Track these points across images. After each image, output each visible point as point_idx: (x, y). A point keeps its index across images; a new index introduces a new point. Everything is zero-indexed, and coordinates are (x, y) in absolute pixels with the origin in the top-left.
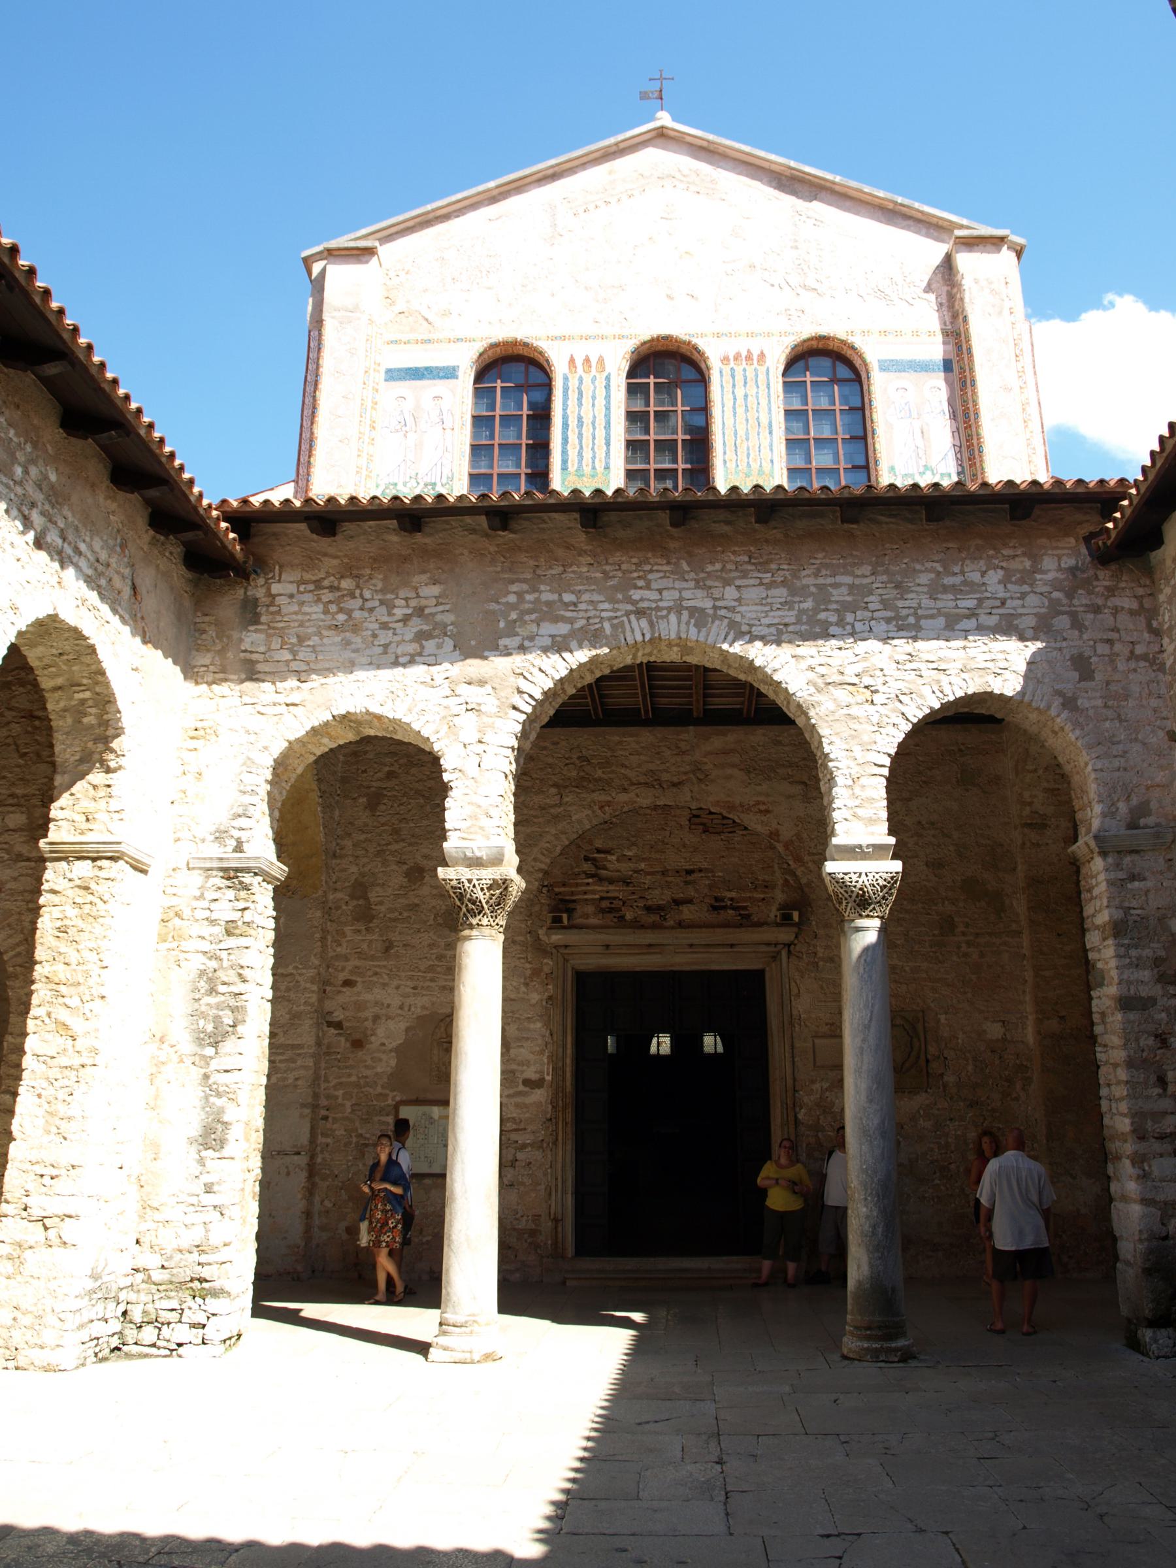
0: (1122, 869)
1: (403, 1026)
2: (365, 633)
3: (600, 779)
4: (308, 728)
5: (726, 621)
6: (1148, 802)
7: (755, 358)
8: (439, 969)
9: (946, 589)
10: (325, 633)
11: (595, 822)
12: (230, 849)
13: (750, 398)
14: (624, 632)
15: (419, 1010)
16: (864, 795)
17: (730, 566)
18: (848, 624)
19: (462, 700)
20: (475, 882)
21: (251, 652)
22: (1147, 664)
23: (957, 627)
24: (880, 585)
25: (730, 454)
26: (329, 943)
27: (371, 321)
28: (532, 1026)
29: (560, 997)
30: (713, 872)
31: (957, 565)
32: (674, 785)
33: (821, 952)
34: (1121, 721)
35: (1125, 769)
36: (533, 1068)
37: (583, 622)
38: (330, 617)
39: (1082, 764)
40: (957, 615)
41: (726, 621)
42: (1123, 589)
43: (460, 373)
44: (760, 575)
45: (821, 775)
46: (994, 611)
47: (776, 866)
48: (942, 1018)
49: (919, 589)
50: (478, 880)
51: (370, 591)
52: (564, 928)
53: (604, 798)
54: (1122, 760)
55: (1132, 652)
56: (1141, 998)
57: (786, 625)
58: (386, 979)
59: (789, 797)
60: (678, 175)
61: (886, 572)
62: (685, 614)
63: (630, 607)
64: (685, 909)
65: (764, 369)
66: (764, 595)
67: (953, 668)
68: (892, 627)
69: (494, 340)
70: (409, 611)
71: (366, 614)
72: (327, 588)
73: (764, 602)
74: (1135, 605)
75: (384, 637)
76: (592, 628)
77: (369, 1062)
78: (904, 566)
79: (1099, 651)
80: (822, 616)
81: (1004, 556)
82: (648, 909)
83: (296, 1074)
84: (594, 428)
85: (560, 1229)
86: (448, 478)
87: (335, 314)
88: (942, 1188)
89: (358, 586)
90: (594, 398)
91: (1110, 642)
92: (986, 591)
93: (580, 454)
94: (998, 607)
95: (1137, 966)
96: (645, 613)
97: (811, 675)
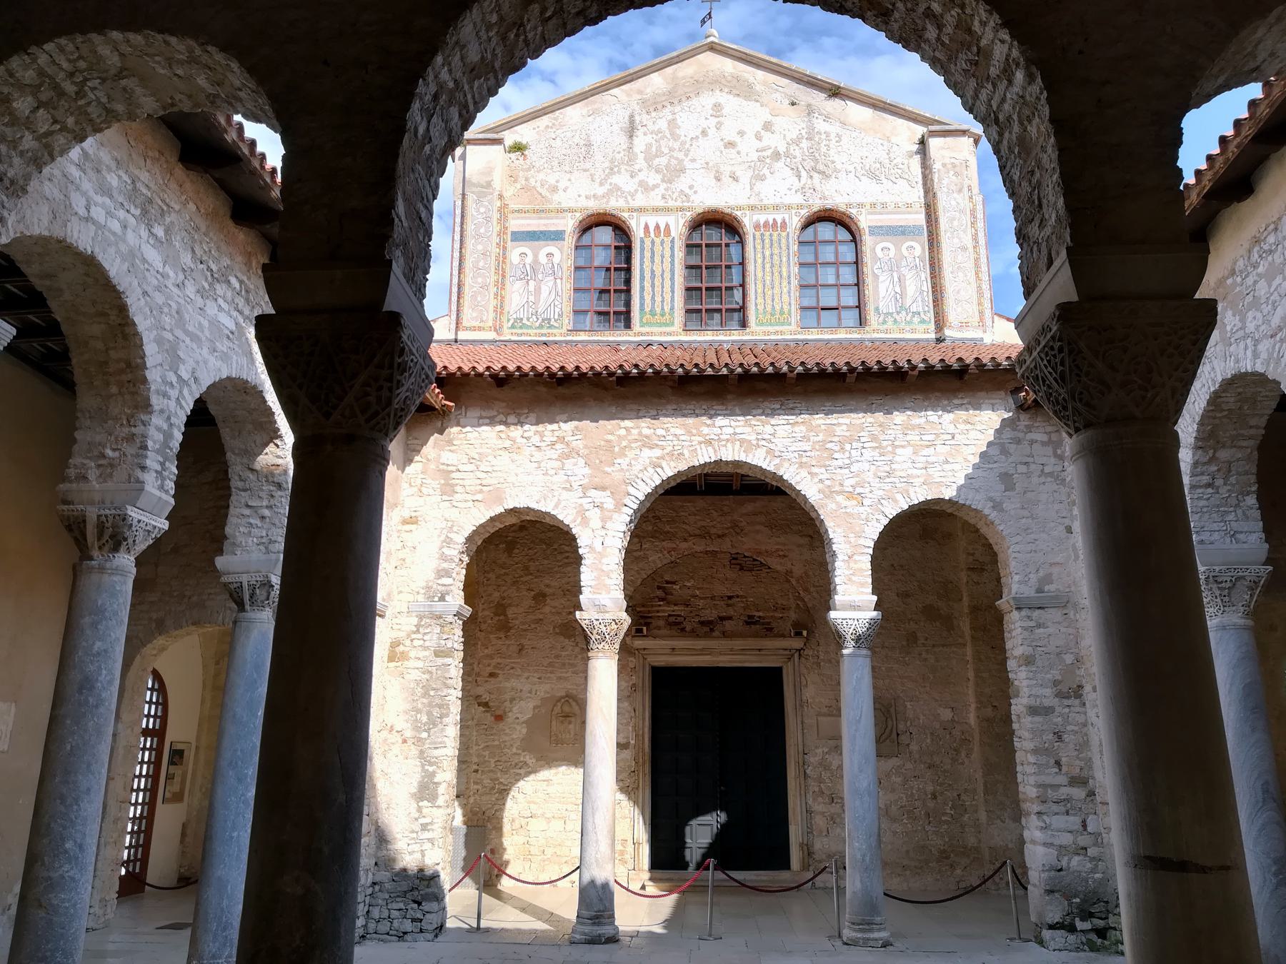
1: (531, 705)
6: (1051, 574)
7: (779, 225)
8: (557, 665)
9: (913, 427)
11: (665, 562)
12: (436, 599)
15: (542, 694)
16: (856, 566)
19: (590, 500)
21: (448, 465)
23: (920, 454)
25: (760, 300)
27: (501, 197)
29: (641, 685)
30: (746, 597)
32: (719, 537)
34: (1033, 519)
35: (1035, 551)
37: (671, 448)
38: (500, 442)
39: (1005, 546)
43: (567, 234)
45: (827, 551)
46: (947, 442)
48: (908, 704)
52: (644, 636)
54: (1034, 545)
55: (1042, 471)
56: (1045, 707)
58: (519, 672)
59: (799, 546)
60: (723, 81)
64: (727, 623)
67: (917, 481)
69: (590, 212)
70: (555, 439)
71: (525, 440)
74: (1045, 438)
75: (538, 456)
77: (507, 731)
80: (829, 445)
82: (702, 623)
84: (663, 280)
86: (559, 315)
87: (474, 189)
90: (663, 257)
93: (653, 298)
97: (821, 486)
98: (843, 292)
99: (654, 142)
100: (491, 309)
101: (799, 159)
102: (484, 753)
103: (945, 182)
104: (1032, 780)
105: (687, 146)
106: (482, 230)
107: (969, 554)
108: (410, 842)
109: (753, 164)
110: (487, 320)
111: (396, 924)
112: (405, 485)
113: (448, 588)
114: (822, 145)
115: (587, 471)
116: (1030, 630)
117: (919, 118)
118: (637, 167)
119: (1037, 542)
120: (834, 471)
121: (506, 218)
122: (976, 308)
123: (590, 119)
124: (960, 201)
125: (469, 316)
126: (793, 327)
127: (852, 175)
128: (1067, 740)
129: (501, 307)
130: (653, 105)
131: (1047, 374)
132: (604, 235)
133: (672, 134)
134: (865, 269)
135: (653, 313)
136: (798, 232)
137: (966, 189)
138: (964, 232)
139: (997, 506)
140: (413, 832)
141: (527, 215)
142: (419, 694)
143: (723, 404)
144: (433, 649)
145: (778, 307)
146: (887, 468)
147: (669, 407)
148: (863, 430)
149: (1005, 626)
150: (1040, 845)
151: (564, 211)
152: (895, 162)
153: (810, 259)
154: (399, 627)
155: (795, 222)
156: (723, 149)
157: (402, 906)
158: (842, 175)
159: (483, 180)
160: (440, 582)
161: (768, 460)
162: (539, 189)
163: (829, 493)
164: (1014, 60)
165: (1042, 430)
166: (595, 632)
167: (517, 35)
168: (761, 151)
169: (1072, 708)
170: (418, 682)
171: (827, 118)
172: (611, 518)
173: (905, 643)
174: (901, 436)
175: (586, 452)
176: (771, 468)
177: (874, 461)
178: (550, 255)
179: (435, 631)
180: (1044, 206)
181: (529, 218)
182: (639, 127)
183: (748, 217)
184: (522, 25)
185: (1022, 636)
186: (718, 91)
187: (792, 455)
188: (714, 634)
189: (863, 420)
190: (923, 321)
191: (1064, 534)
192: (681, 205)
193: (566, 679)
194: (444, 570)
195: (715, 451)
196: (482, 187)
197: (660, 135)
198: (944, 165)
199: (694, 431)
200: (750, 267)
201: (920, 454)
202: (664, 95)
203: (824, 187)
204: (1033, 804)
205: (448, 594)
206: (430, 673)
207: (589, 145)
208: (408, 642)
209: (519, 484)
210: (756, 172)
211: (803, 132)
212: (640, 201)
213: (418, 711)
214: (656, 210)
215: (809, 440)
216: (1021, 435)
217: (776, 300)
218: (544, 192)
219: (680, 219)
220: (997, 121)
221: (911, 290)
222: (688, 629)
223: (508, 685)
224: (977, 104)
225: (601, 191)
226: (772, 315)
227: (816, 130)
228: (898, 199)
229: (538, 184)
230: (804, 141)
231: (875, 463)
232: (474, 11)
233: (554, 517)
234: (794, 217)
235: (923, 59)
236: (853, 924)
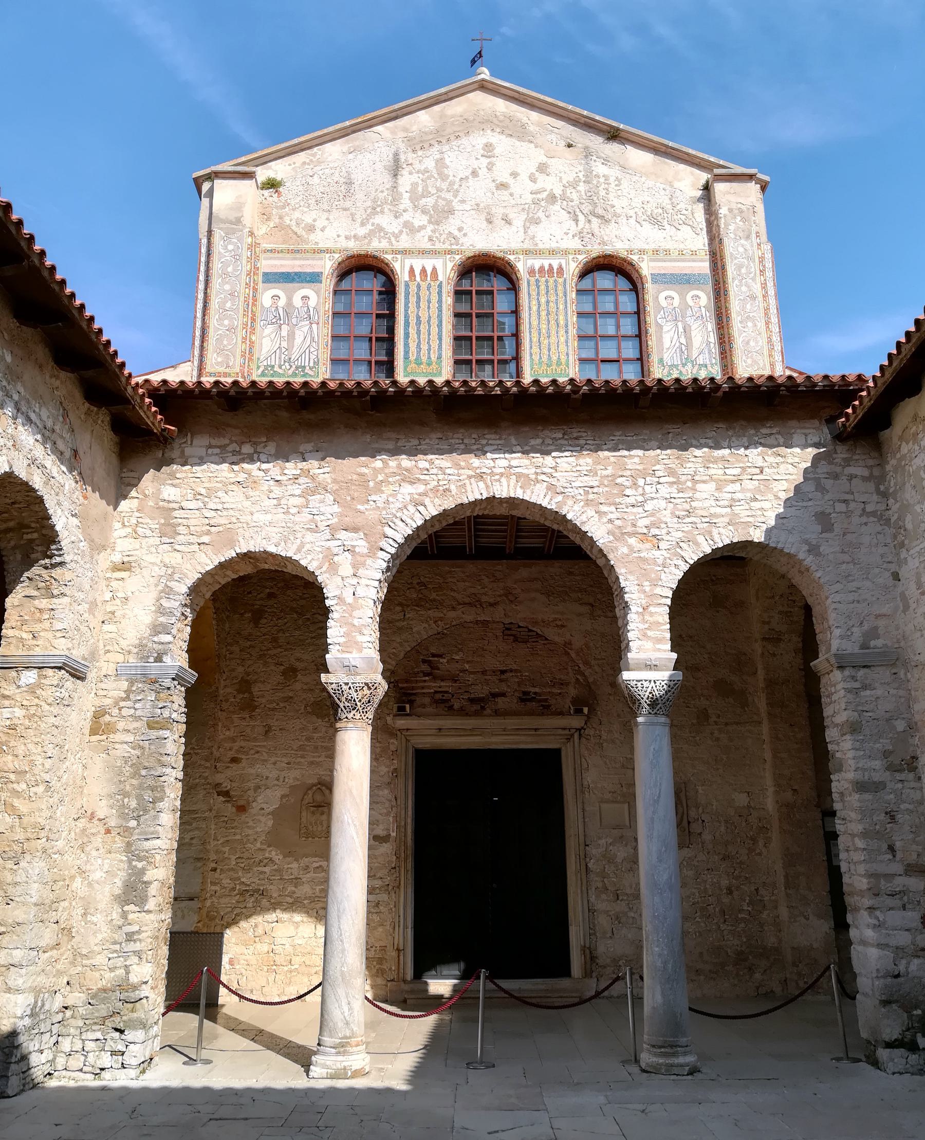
0: (857, 680)
1: (278, 793)
3: (435, 600)
4: (216, 563)
6: (876, 628)
7: (555, 271)
8: (308, 748)
12: (152, 659)
13: (551, 304)
15: (291, 781)
18: (639, 486)
19: (339, 543)
20: (350, 684)
21: (169, 502)
22: (876, 520)
23: (725, 490)
25: (535, 350)
26: (220, 728)
27: (251, 234)
28: (381, 793)
29: (403, 770)
32: (491, 605)
33: (604, 735)
35: (858, 602)
36: (381, 827)
38: (232, 475)
39: (823, 597)
41: (545, 484)
42: (857, 460)
45: (616, 604)
46: (754, 477)
47: (569, 668)
48: (700, 789)
50: (353, 683)
52: (407, 715)
53: (439, 614)
54: (856, 594)
55: (864, 510)
56: (875, 783)
58: (265, 756)
59: (580, 615)
60: (495, 121)
64: (500, 700)
67: (722, 521)
69: (350, 253)
70: (298, 472)
71: (262, 474)
72: (231, 452)
73: (574, 470)
74: (866, 473)
75: (277, 491)
77: (251, 824)
79: (837, 510)
80: (619, 480)
82: (472, 701)
83: (191, 834)
84: (430, 327)
85: (401, 957)
86: (314, 362)
87: (222, 226)
88: (702, 924)
89: (256, 452)
90: (429, 302)
91: (845, 501)
95: (870, 757)
97: (610, 526)
98: (624, 344)
99: (420, 182)
101: (576, 202)
102: (224, 849)
103: (732, 227)
104: (861, 869)
105: (455, 187)
106: (230, 269)
107: (764, 623)
108: (110, 956)
109: (527, 206)
110: (234, 364)
111: (91, 1058)
112: (117, 525)
113: (166, 647)
115: (336, 509)
116: (855, 692)
117: (702, 164)
118: (402, 207)
119: (860, 591)
120: (626, 510)
121: (257, 258)
122: (767, 360)
123: (351, 156)
124: (748, 247)
125: (214, 361)
128: (900, 821)
129: (250, 352)
130: (420, 143)
133: (440, 174)
134: (648, 319)
135: (418, 362)
136: (575, 279)
137: (754, 236)
138: (754, 279)
139: (814, 550)
140: (115, 943)
141: (280, 255)
142: (127, 774)
143: (495, 433)
144: (145, 719)
145: (554, 358)
146: (687, 507)
147: (434, 436)
149: (822, 690)
150: (873, 946)
151: (321, 251)
152: (678, 207)
153: (588, 308)
154: (105, 693)
155: (573, 268)
156: (495, 191)
157: (99, 1035)
159: (232, 216)
160: (156, 639)
161: (548, 497)
163: (620, 535)
165: (861, 463)
166: (343, 699)
168: (536, 193)
169: (906, 783)
170: (126, 760)
171: (606, 161)
172: (364, 564)
173: (695, 721)
174: (702, 470)
175: (336, 487)
176: (553, 506)
177: (669, 500)
178: (305, 298)
179: (149, 698)
182: (404, 166)
183: (521, 262)
185: (845, 700)
186: (489, 131)
187: (576, 492)
188: (485, 712)
191: (890, 582)
192: (449, 247)
193: (318, 764)
194: (161, 624)
195: (487, 487)
196: (231, 223)
197: (426, 175)
198: (730, 210)
200: (525, 315)
201: (725, 490)
203: (603, 232)
204: (863, 897)
205: (166, 654)
206: (143, 748)
207: (349, 183)
208: (115, 711)
209: (255, 524)
210: (531, 215)
211: (581, 175)
212: (404, 242)
213: (126, 795)
214: (423, 253)
216: (838, 469)
217: (552, 350)
218: (300, 231)
219: (448, 262)
221: (698, 340)
222: (456, 706)
223: (252, 771)
225: (362, 231)
226: (548, 366)
227: (594, 173)
228: (682, 246)
229: (293, 223)
230: (581, 184)
231: (672, 500)
233: (296, 563)
234: (571, 262)
236: (654, 1046)
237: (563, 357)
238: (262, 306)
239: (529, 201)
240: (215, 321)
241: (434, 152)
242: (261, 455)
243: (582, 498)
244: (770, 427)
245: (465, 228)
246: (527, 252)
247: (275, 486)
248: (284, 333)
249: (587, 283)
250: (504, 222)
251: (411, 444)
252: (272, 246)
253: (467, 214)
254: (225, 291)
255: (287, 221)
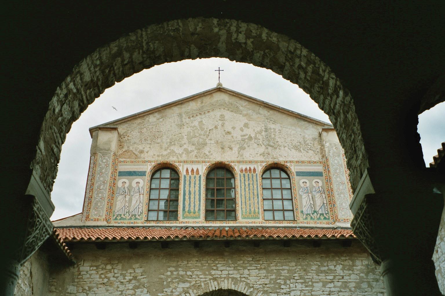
2: (115, 286)
5: (245, 283)
7: (252, 170)
9: (322, 272)
10: (99, 286)
13: (251, 185)
14: (208, 287)
17: (246, 262)
18: (288, 284)
23: (327, 286)
24: (298, 270)
25: (244, 206)
31: (325, 263)
37: (194, 282)
38: (101, 280)
40: (327, 282)
41: (245, 283)
43: (147, 174)
44: (256, 265)
46: (340, 280)
49: (312, 272)
51: (117, 270)
57: (266, 284)
61: (301, 265)
62: (230, 279)
63: (211, 277)
65: (255, 175)
66: (258, 273)
68: (303, 286)
69: (159, 162)
70: (131, 278)
71: (115, 279)
73: (258, 276)
75: (121, 288)
76: (197, 285)
78: (307, 263)
80: (279, 281)
81: (342, 260)
84: (195, 195)
86: (141, 213)
89: (112, 268)
90: (195, 184)
92: (336, 273)
93: (190, 204)
94: (341, 279)
96: (216, 279)
99: (192, 131)
100: (105, 209)
103: (332, 152)
106: (103, 171)
109: (239, 142)
110: (102, 215)
114: (272, 134)
123: (161, 120)
126: (261, 220)
127: (286, 148)
131: (365, 230)
132: (166, 174)
133: (201, 128)
135: (189, 212)
138: (342, 175)
143: (222, 258)
145: (252, 210)
147: (194, 259)
148: (295, 273)
152: (307, 142)
155: (260, 169)
158: (282, 148)
159: (107, 147)
161: (246, 289)
162: (134, 152)
164: (338, 86)
167: (110, 71)
171: (274, 122)
177: (301, 291)
180: (357, 150)
181: (129, 165)
184: (112, 66)
189: (296, 267)
190: (325, 218)
192: (204, 160)
195: (218, 284)
196: (105, 150)
197: (195, 128)
198: (331, 144)
199: (207, 273)
202: (197, 110)
203: (273, 153)
210: (241, 146)
212: (184, 158)
215: (267, 278)
218: (137, 153)
219: (204, 166)
220: (334, 113)
224: (325, 106)
225: (165, 153)
228: (309, 160)
229: (134, 149)
230: (263, 132)
231: (303, 291)
232: (88, 59)
234: (259, 166)
235: (300, 87)
237: (257, 210)
238: (118, 187)
239: (240, 139)
240: (95, 194)
241: (198, 118)
242: (115, 270)
243: (262, 289)
244: (346, 256)
245: (212, 151)
246: (239, 162)
247: (120, 284)
248: (127, 199)
249: (267, 175)
250: (229, 148)
251: (184, 263)
252: (124, 159)
253: (212, 145)
254: (100, 181)
255: (131, 148)
